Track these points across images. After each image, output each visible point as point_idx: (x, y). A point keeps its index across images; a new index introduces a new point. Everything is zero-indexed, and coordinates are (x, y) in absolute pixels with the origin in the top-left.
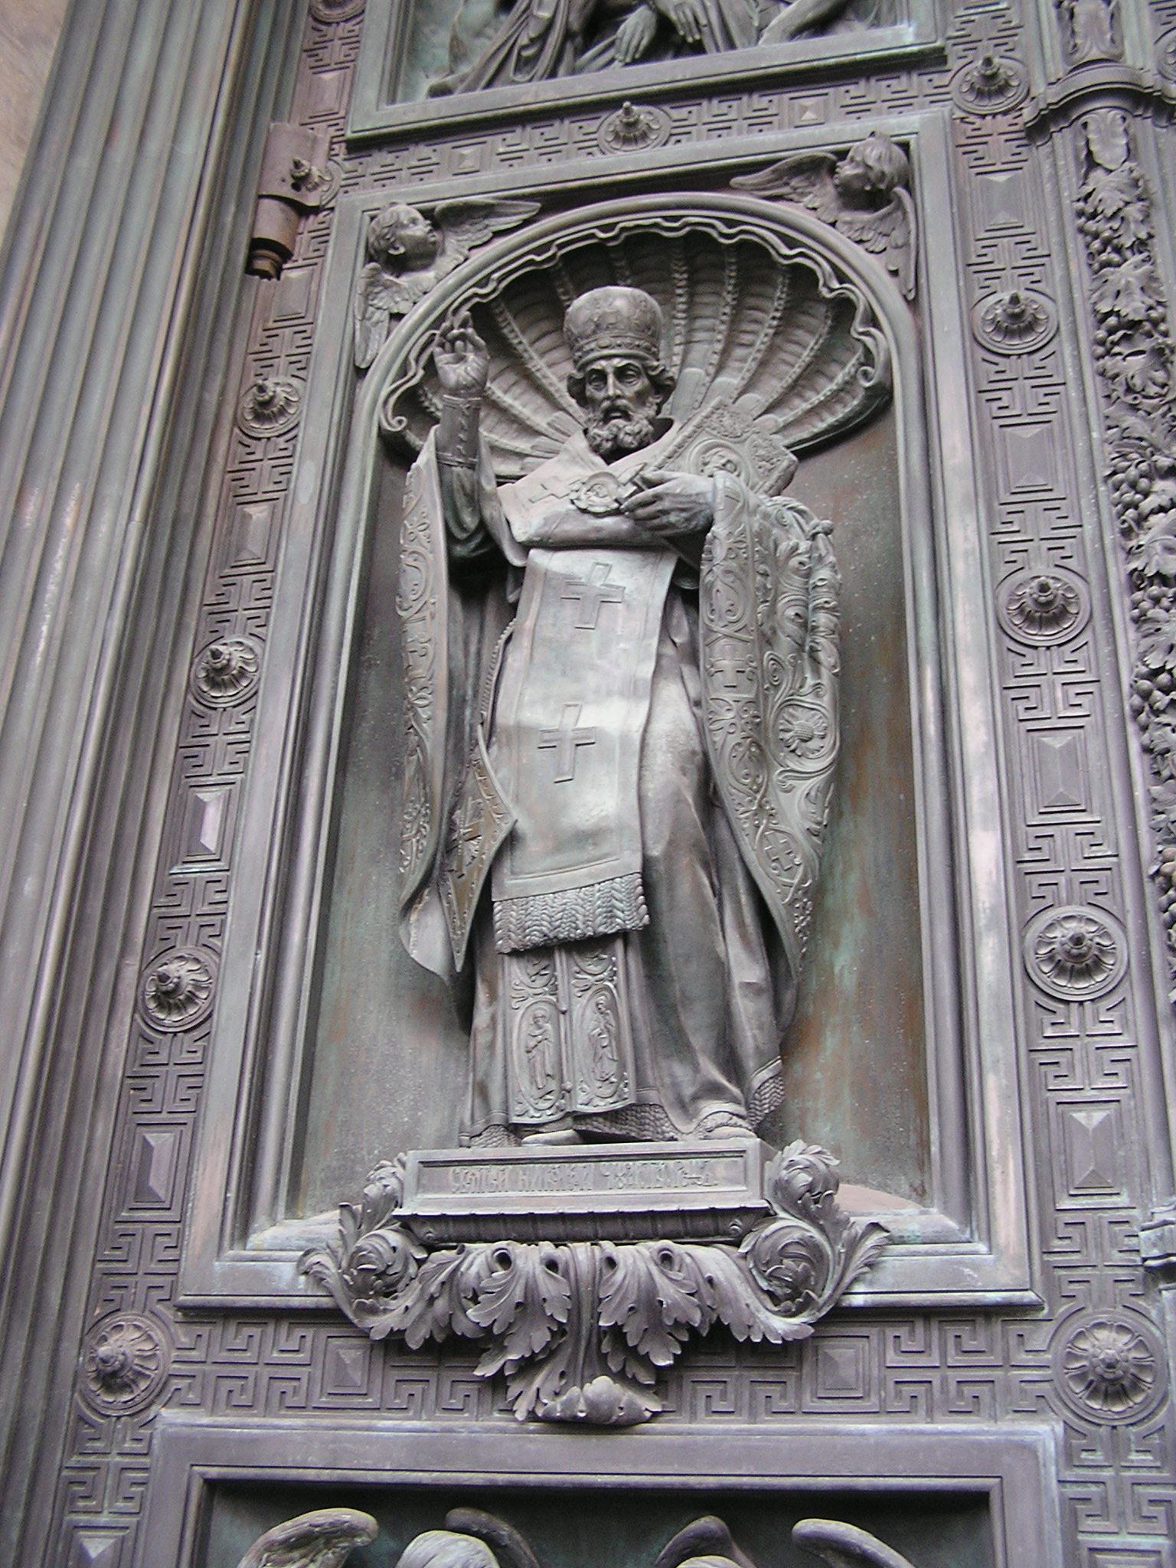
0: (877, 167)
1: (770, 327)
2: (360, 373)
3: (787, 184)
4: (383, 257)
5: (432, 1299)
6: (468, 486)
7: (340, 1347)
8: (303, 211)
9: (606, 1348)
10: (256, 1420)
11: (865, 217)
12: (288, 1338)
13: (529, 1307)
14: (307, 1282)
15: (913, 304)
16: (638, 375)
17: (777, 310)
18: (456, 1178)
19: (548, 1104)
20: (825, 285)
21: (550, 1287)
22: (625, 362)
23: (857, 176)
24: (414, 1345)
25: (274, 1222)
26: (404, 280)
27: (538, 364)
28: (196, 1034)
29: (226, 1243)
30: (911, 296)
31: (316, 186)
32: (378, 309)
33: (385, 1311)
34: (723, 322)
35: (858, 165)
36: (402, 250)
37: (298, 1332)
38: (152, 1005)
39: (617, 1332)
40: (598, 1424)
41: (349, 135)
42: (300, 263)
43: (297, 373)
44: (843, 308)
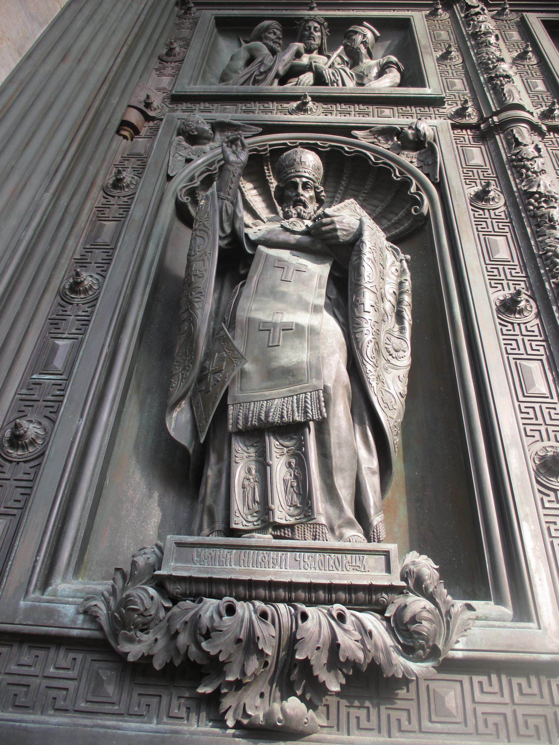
2: (169, 178)
5: (177, 633)
6: (230, 211)
7: (100, 668)
8: (148, 118)
9: (295, 675)
10: (32, 717)
12: (64, 658)
14: (84, 621)
16: (311, 188)
17: (366, 189)
18: (199, 556)
19: (256, 519)
22: (307, 180)
24: (157, 665)
25: (64, 580)
28: (32, 464)
29: (32, 588)
31: (155, 109)
32: (181, 155)
33: (140, 641)
35: (413, 130)
36: (196, 133)
37: (71, 655)
38: (6, 445)
41: (173, 92)
42: (143, 136)
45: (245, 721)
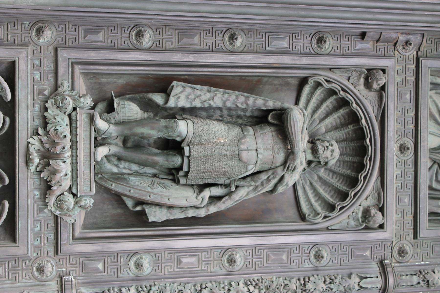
0: (372, 221)
1: (335, 184)
3: (376, 192)
4: (369, 75)
8: (395, 44)
11: (360, 215)
13: (54, 144)
15: (327, 229)
20: (340, 204)
21: (58, 149)
23: (370, 214)
26: (362, 80)
27: (336, 116)
30: (329, 228)
34: (340, 170)
36: (370, 81)
39: (49, 164)
40: (28, 161)
43: (333, 49)
44: (331, 208)
45: (30, 145)
